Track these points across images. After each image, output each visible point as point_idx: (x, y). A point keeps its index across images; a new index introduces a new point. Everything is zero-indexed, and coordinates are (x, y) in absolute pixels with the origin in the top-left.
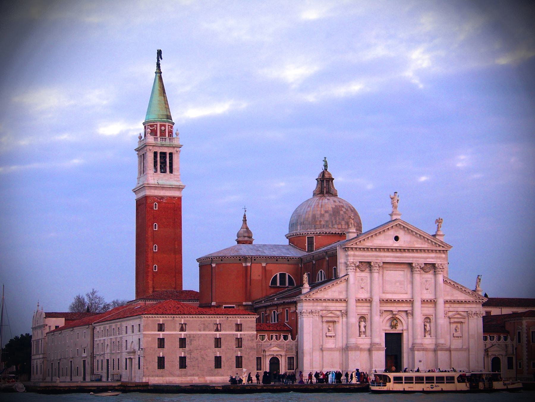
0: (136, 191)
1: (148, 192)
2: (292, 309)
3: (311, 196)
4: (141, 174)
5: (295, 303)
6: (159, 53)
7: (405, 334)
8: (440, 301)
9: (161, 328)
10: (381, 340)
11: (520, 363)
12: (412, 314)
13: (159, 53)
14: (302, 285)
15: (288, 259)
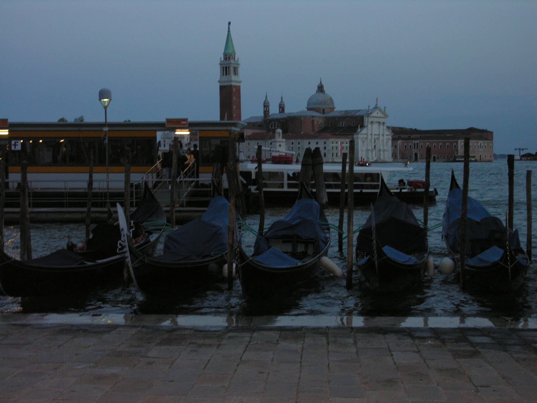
0: (219, 82)
1: (233, 84)
2: (350, 137)
3: (315, 92)
4: (223, 75)
5: (353, 135)
6: (229, 23)
7: (377, 145)
8: (385, 135)
9: (333, 143)
10: (373, 148)
11: (396, 156)
12: (379, 139)
13: (229, 23)
14: (358, 128)
15: (323, 117)
